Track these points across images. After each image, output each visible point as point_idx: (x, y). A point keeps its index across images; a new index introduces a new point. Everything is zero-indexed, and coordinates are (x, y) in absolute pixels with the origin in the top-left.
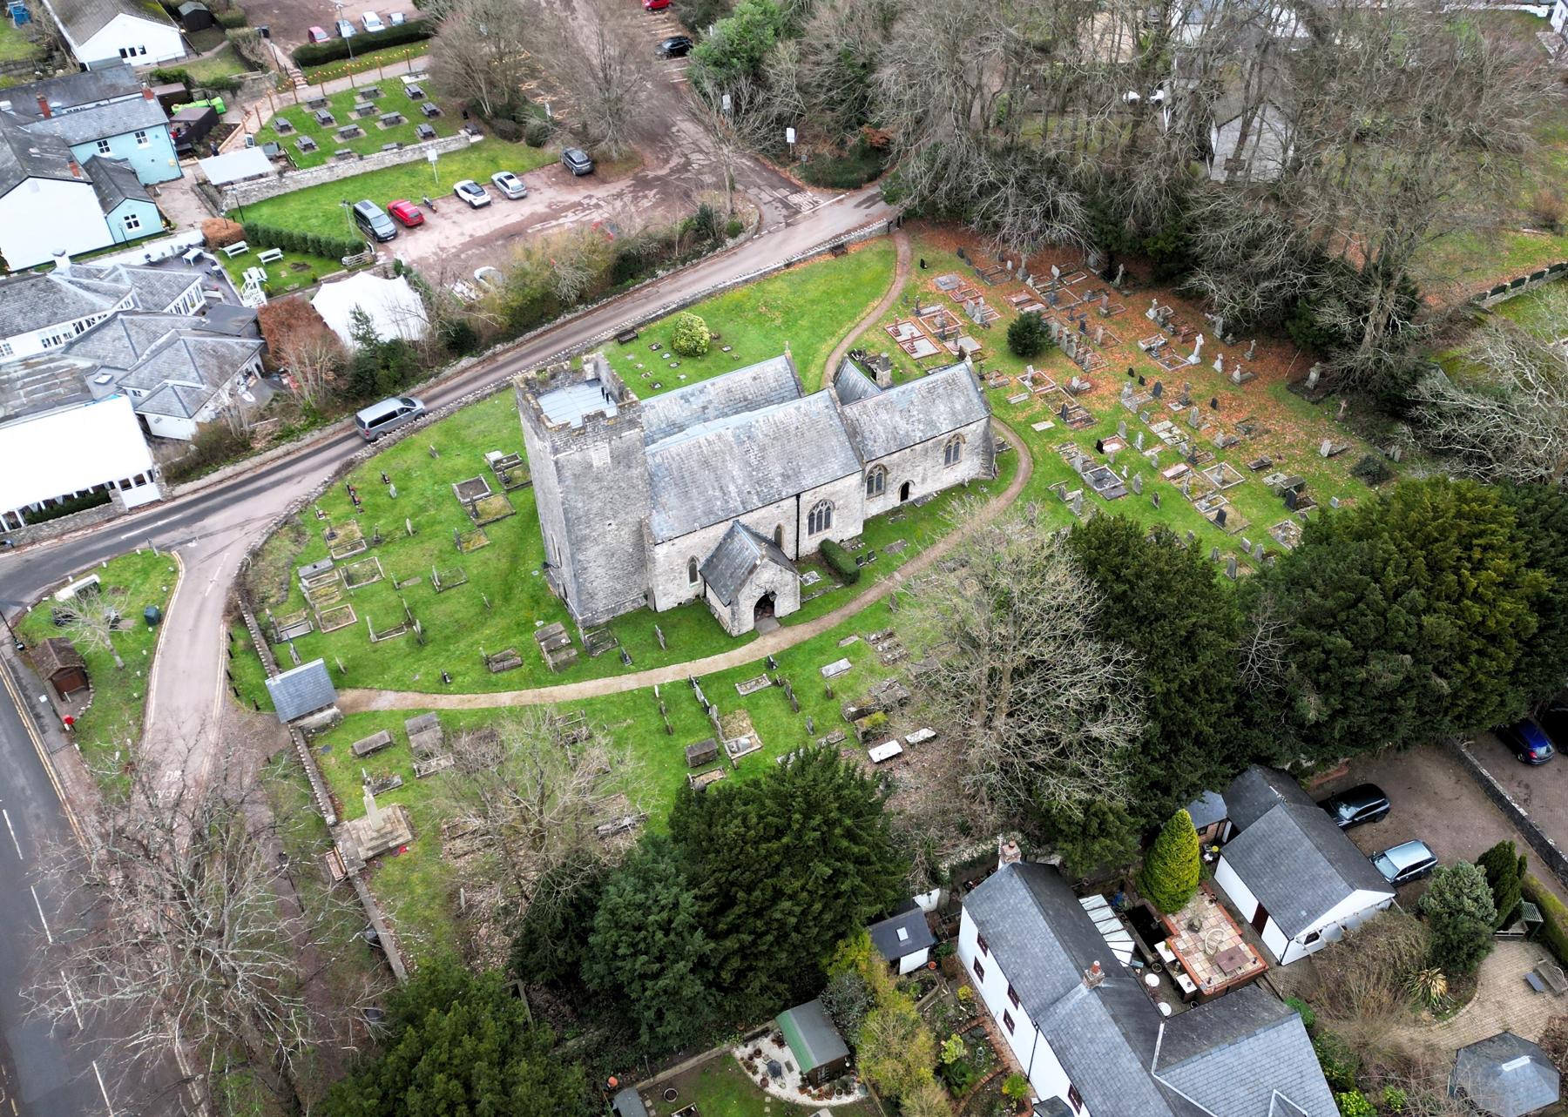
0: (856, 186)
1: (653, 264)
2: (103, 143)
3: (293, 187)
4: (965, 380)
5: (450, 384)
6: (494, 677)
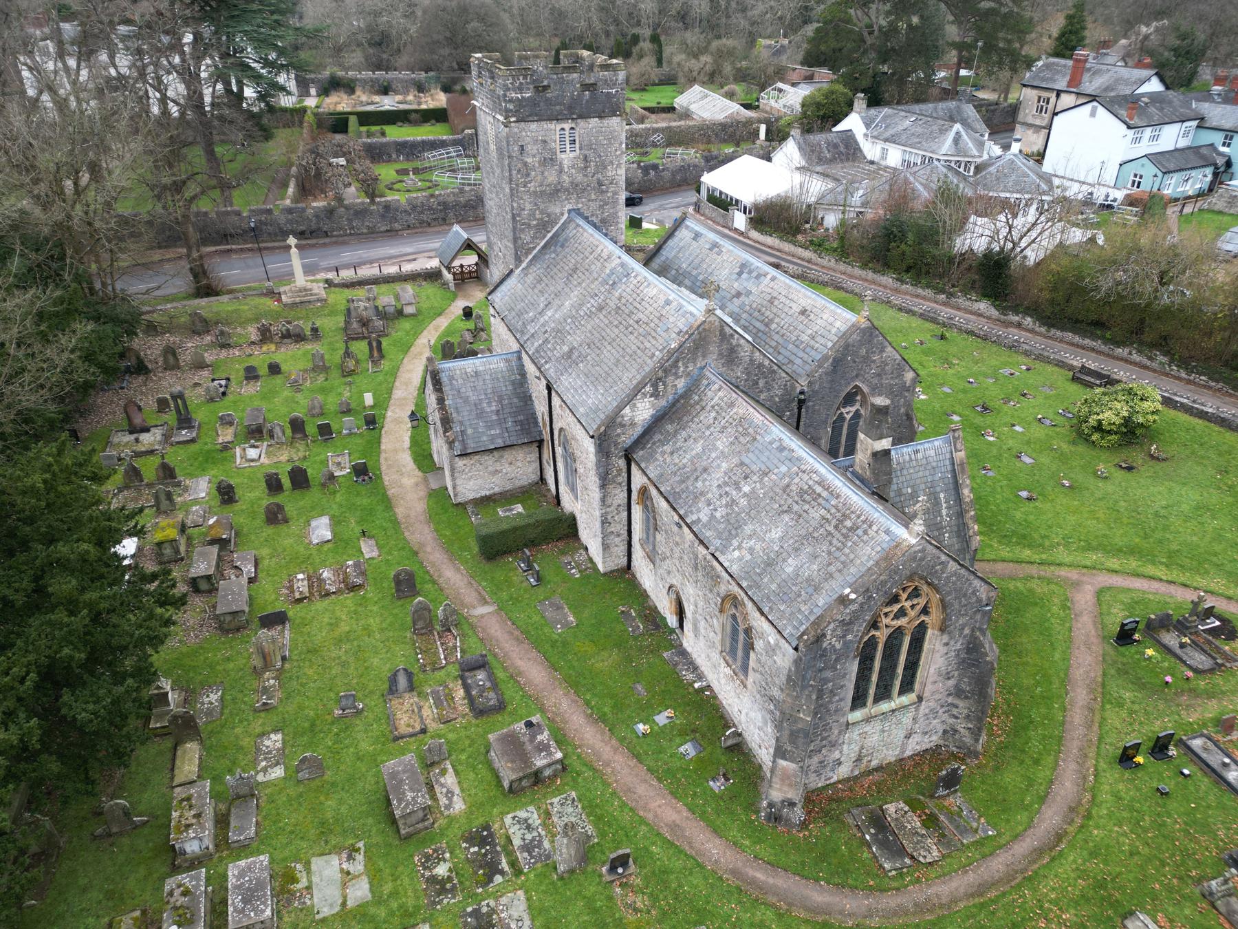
4: (867, 555)
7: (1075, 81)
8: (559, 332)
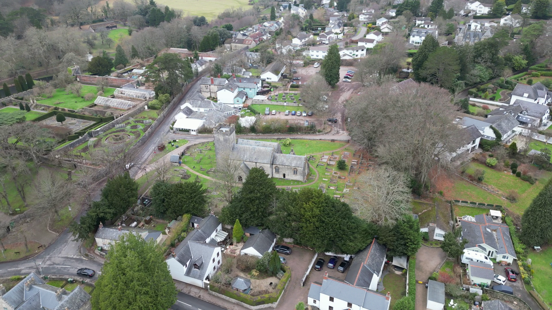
1: (298, 131)
2: (244, 88)
3: (264, 103)
4: (303, 159)
7: (212, 83)
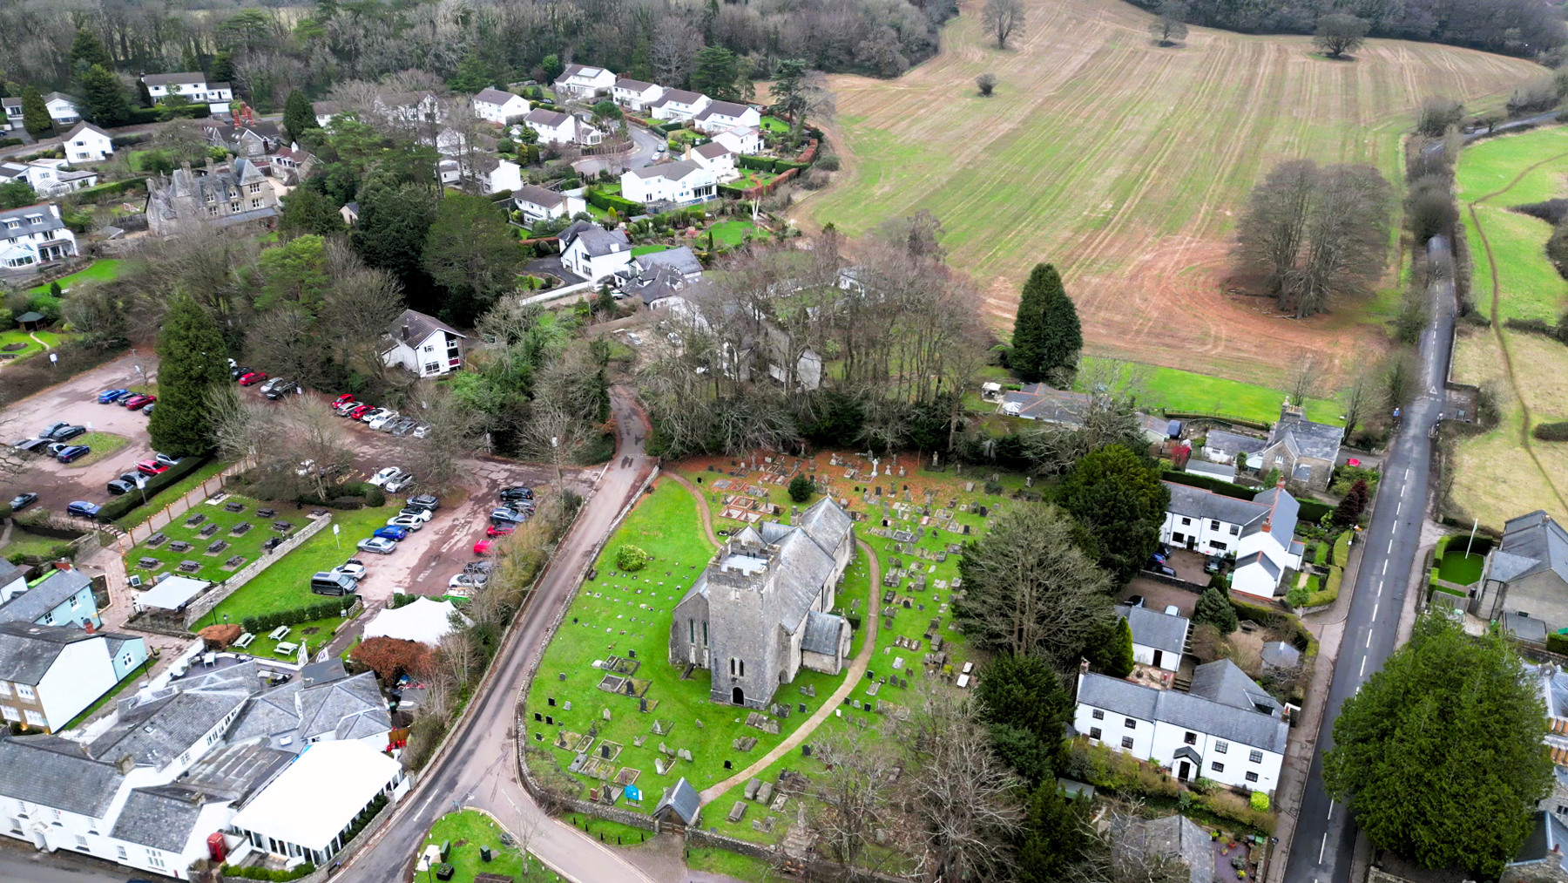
0: (609, 458)
5: (510, 645)
6: (751, 753)
8: (807, 585)
